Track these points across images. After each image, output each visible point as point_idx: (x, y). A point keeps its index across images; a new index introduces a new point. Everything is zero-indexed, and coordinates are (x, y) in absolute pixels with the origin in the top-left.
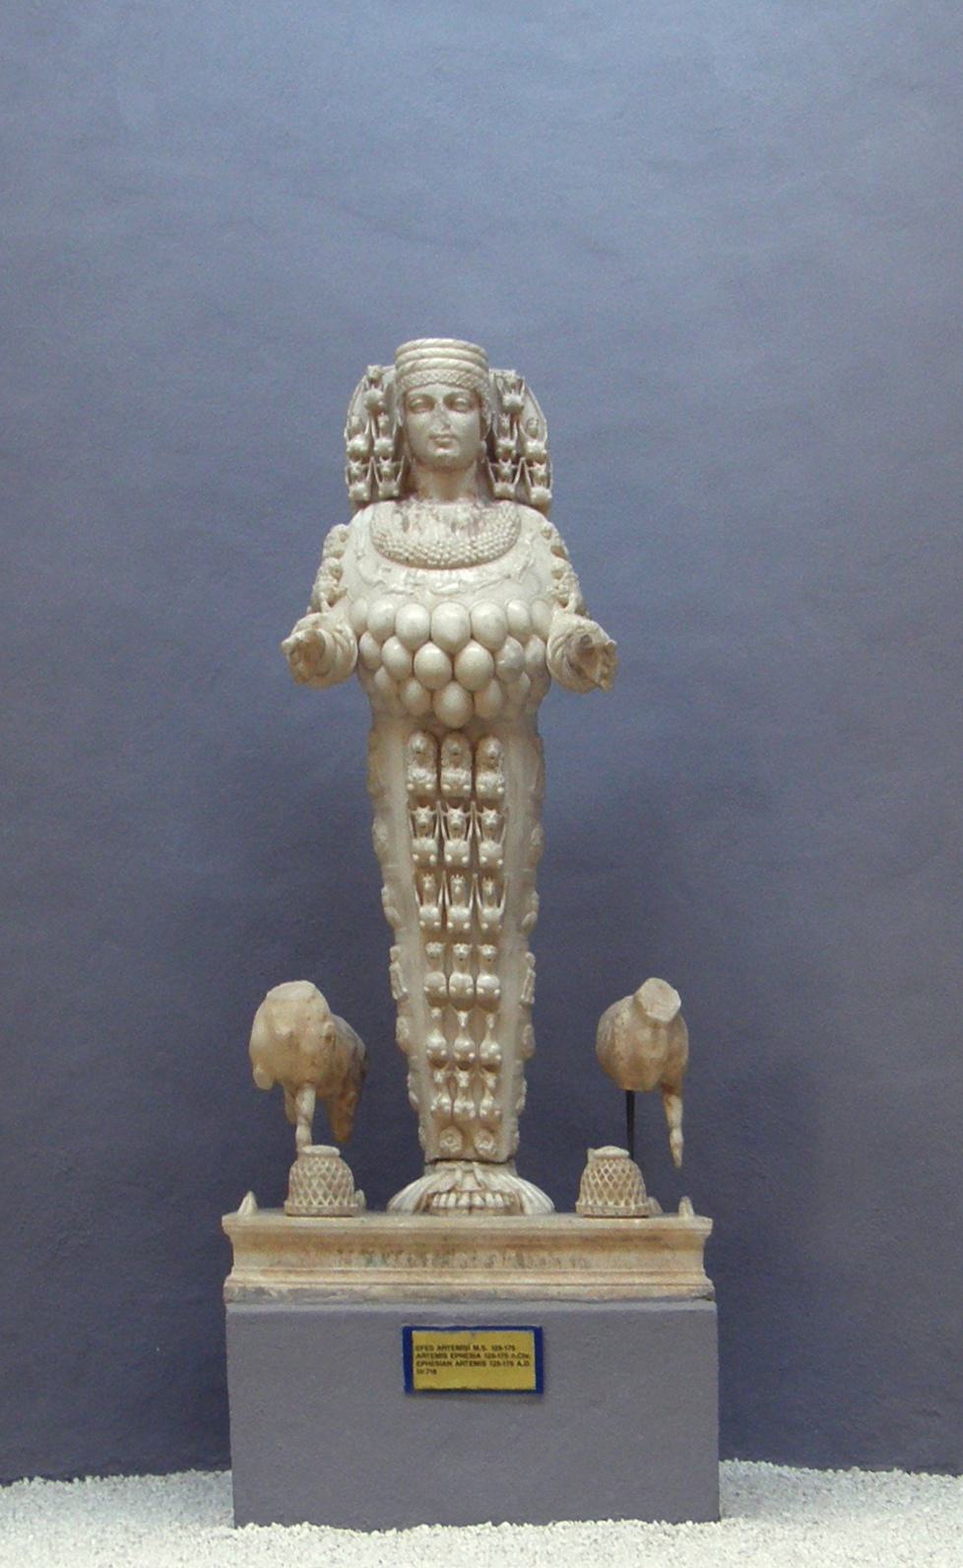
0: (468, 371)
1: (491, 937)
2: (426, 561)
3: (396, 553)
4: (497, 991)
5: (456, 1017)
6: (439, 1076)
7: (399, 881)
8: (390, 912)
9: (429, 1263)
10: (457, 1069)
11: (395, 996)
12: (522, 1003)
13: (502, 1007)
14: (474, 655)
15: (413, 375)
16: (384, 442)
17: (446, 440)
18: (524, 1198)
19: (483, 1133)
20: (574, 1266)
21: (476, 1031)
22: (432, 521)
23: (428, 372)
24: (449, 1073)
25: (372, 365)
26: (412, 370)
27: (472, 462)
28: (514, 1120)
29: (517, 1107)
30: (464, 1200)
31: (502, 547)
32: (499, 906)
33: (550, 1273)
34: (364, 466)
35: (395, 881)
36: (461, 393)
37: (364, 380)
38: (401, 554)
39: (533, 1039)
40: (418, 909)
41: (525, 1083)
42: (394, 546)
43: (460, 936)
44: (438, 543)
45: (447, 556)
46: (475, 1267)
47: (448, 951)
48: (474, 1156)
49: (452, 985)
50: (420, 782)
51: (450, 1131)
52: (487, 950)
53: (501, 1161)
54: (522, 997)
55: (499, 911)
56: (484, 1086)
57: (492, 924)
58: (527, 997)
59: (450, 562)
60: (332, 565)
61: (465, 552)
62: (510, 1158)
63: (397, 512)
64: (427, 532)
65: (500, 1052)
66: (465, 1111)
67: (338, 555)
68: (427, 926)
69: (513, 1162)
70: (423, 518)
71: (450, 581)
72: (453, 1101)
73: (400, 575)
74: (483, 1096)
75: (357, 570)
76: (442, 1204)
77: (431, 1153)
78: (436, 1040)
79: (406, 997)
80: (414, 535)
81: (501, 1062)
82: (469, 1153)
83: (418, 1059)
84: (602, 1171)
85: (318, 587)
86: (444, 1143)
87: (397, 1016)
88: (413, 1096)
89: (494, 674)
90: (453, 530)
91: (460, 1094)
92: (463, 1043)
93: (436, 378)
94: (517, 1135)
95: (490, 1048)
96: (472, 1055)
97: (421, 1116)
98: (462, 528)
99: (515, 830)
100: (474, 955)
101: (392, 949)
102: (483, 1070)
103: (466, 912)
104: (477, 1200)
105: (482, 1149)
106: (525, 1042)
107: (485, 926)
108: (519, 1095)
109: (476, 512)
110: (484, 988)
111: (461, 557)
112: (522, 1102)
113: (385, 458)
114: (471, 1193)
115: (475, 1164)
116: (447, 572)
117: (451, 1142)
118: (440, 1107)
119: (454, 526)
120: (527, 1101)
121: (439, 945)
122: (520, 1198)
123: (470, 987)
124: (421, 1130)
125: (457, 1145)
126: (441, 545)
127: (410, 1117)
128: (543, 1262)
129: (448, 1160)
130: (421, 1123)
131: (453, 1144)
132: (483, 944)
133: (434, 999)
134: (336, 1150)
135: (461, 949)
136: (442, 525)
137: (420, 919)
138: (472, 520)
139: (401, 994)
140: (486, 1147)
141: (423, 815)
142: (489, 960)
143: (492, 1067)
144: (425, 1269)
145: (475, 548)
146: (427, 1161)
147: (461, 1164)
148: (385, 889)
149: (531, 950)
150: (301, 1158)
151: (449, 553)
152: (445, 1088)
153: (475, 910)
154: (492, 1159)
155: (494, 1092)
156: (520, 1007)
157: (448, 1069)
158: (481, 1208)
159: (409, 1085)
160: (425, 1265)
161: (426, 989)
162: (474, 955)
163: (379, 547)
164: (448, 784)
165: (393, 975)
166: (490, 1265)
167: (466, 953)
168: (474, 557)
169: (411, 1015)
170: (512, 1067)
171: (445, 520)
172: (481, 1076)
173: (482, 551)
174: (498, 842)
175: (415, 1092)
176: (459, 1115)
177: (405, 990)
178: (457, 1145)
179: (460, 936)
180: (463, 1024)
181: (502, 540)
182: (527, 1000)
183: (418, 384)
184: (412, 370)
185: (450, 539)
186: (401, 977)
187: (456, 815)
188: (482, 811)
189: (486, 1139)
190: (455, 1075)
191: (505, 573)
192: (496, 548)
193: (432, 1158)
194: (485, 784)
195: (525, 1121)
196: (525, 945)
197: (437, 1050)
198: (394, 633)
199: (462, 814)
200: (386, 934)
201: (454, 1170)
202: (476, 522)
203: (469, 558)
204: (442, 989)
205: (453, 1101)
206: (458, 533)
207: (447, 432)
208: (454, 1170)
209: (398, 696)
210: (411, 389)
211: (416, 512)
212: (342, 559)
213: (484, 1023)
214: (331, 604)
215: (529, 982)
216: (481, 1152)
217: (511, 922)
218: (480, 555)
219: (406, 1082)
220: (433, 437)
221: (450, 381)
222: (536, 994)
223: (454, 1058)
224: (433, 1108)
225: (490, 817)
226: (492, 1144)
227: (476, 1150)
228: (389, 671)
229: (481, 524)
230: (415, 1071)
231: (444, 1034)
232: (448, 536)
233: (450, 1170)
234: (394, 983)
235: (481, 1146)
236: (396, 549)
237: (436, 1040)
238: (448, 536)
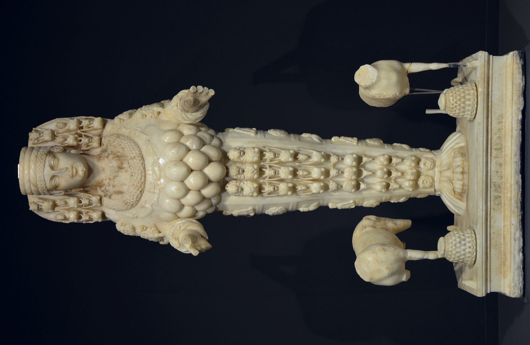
0: (37, 157)
1: (327, 157)
2: (142, 182)
3: (137, 198)
7: (298, 203)
8: (312, 207)
9: (499, 195)
12: (358, 143)
14: (192, 160)
15: (39, 186)
16: (72, 202)
17: (74, 171)
18: (457, 146)
20: (502, 122)
22: (118, 178)
25: (29, 207)
27: (84, 158)
28: (414, 149)
30: (460, 177)
31: (133, 144)
33: (505, 135)
34: (84, 213)
35: (298, 204)
36: (49, 161)
37: (36, 212)
38: (138, 195)
39: (374, 139)
40: (314, 194)
41: (395, 144)
44: (132, 176)
46: (501, 172)
50: (252, 189)
54: (355, 144)
55: (315, 153)
57: (323, 157)
59: (143, 170)
60: (140, 231)
61: (137, 162)
63: (110, 197)
65: (383, 155)
66: (412, 174)
67: (134, 229)
70: (116, 183)
71: (153, 170)
73: (146, 196)
76: (461, 187)
79: (355, 202)
80: (125, 188)
84: (452, 106)
85: (151, 238)
87: (362, 207)
88: (402, 200)
89: (199, 150)
90: (124, 168)
94: (421, 149)
97: (412, 197)
98: (122, 164)
99: (275, 144)
104: (460, 170)
108: (402, 147)
109: (111, 156)
111: (140, 164)
112: (405, 146)
113: (80, 202)
114: (453, 173)
116: (147, 172)
119: (120, 168)
122: (456, 149)
124: (419, 197)
126: (134, 174)
127: (412, 202)
128: (499, 138)
133: (357, 187)
134: (441, 239)
136: (120, 174)
138: (117, 158)
141: (268, 188)
144: (503, 197)
145: (135, 157)
148: (302, 209)
149: (330, 138)
150: (445, 256)
156: (359, 144)
158: (463, 168)
159: (396, 202)
160: (500, 197)
161: (353, 190)
163: (132, 206)
164: (254, 175)
165: (344, 207)
166: (501, 165)
168: (140, 158)
169: (363, 199)
170: (388, 150)
171: (118, 172)
173: (136, 154)
174: (281, 152)
177: (351, 201)
181: (129, 144)
184: (36, 186)
185: (129, 169)
186: (345, 203)
187: (268, 172)
188: (266, 160)
191: (148, 142)
192: (134, 147)
194: (253, 157)
195: (414, 145)
196: (328, 141)
198: (179, 199)
199: (268, 169)
200: (323, 210)
202: (118, 156)
203: (140, 161)
206: (124, 166)
207: (70, 169)
209: (210, 199)
210: (46, 187)
211: (111, 187)
212: (136, 226)
214: (160, 232)
217: (319, 147)
218: (138, 155)
219: (394, 203)
220: (73, 176)
221: (43, 167)
222: (352, 137)
224: (411, 190)
225: (268, 155)
228: (198, 204)
229: (119, 154)
230: (390, 198)
232: (127, 171)
236: (135, 197)
238: (127, 171)
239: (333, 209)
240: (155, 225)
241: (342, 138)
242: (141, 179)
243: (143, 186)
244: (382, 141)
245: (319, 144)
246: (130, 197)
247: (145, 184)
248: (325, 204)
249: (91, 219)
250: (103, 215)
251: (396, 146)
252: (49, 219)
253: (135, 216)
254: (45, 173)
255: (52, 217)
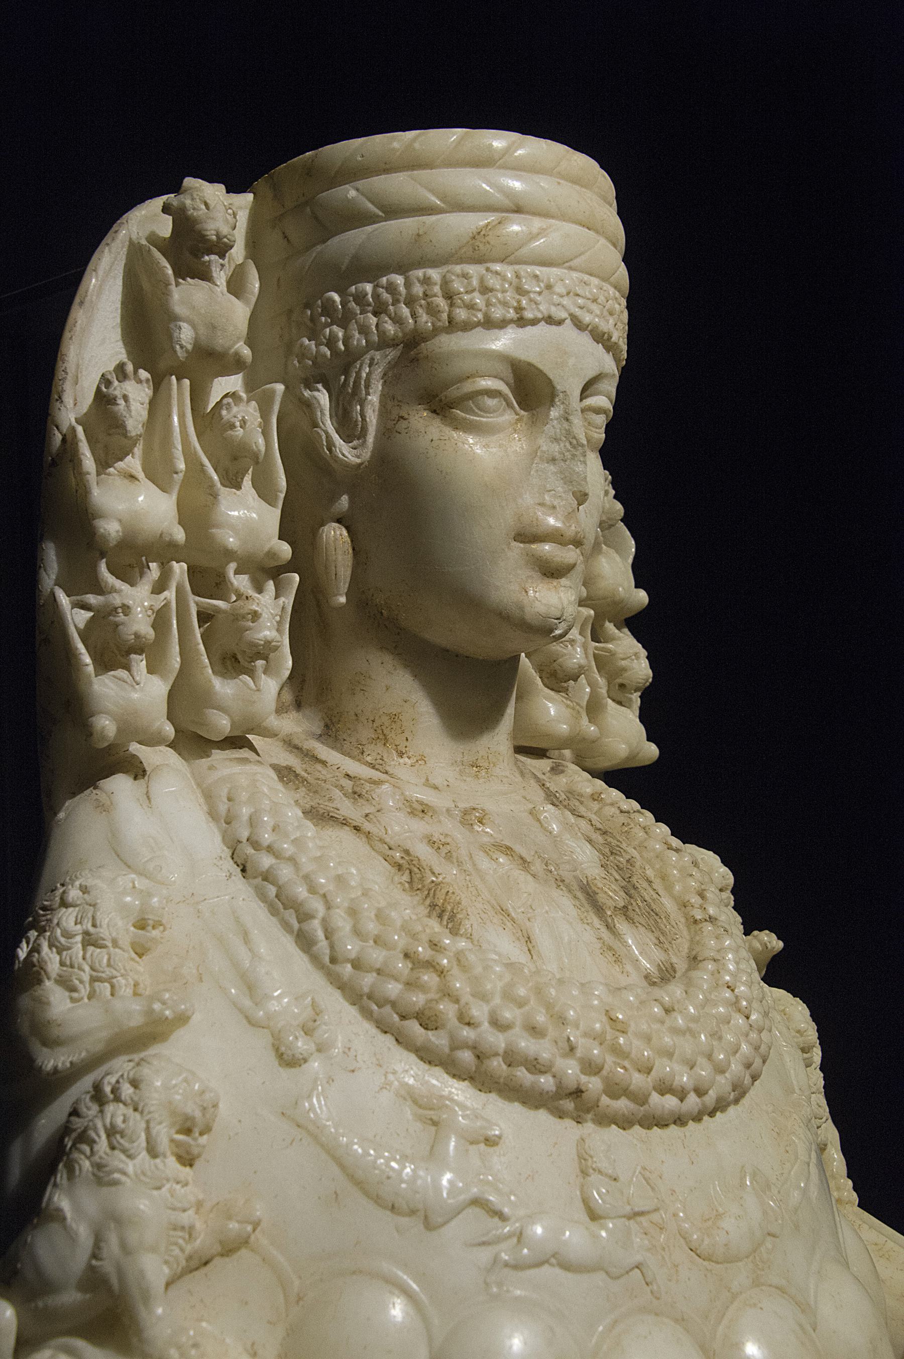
2: (641, 1099)
15: (472, 270)
23: (538, 270)
26: (476, 251)
38: (536, 1066)
42: (497, 1024)
45: (704, 1072)
59: (711, 1097)
64: (543, 941)
75: (312, 1132)
93: (565, 301)
136: (566, 902)
151: (709, 1057)
183: (497, 313)
210: (453, 326)
240: (230, 1248)
242: (664, 1088)
243: (623, 1105)
246: (508, 996)
247: (625, 1122)
249: (114, 653)
250: (115, 761)
252: (78, 316)
253: (302, 1045)
254: (567, 330)
255: (94, 342)
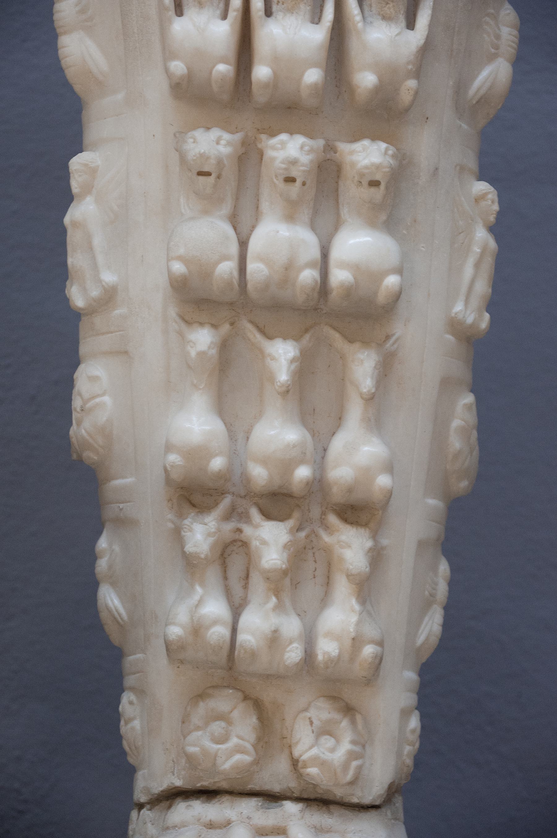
1: (383, 115)
4: (392, 280)
5: (261, 354)
6: (200, 534)
10: (254, 513)
11: (77, 297)
12: (455, 326)
13: (398, 329)
19: (322, 712)
21: (315, 399)
24: (229, 527)
29: (420, 640)
32: (411, 25)
41: (444, 567)
43: (287, 110)
47: (248, 157)
48: (293, 784)
49: (260, 258)
51: (223, 702)
52: (368, 155)
53: (367, 800)
56: (329, 566)
58: (471, 312)
62: (392, 791)
65: (389, 468)
66: (274, 640)
68: (190, 77)
69: (399, 801)
72: (236, 611)
74: (325, 600)
77: (156, 773)
78: (195, 424)
79: (109, 297)
81: (389, 495)
82: (276, 774)
83: (137, 488)
86: (200, 742)
88: (110, 599)
91: (258, 584)
92: (277, 434)
94: (414, 722)
95: (357, 453)
96: (303, 473)
97: (131, 660)
100: (328, 174)
101: (77, 162)
102: (332, 519)
103: (316, 35)
105: (317, 761)
106: (456, 443)
107: (366, 80)
108: (428, 604)
110: (355, 268)
112: (432, 625)
115: (291, 807)
117: (222, 740)
118: (197, 630)
120: (446, 625)
121: (226, 136)
123: (311, 265)
125: (239, 750)
129: (208, 794)
130: (130, 681)
131: (226, 743)
132: (355, 139)
135: (290, 149)
137: (169, 54)
139: (95, 293)
140: (328, 756)
142: (374, 184)
143: (357, 511)
146: (140, 796)
147: (248, 806)
152: (213, 575)
153: (339, 33)
154: (339, 793)
155: (366, 588)
157: (227, 517)
159: (102, 565)
161: (178, 268)
162: (328, 174)
165: (74, 238)
167: (305, 159)
172: (326, 538)
175: (114, 584)
176: (253, 654)
177: (109, 277)
178: (239, 750)
179: (287, 110)
180: (283, 376)
182: (470, 320)
186: (98, 241)
189: (326, 730)
190: (248, 530)
193: (159, 785)
196: (472, 163)
197: (197, 454)
201: (227, 824)
204: (227, 268)
205: (236, 611)
208: (227, 824)
213: (341, 382)
215: (477, 265)
216: (313, 771)
222: (492, 305)
223: (246, 479)
224: (175, 631)
226: (345, 746)
227: (295, 763)
230: (124, 523)
231: (221, 408)
233: (211, 826)
234: (75, 260)
235: (314, 751)
237: (195, 424)
239: (64, 176)
241: (492, 244)
244: (463, 485)
245: (460, 87)
248: (101, 123)
251: (434, 569)
